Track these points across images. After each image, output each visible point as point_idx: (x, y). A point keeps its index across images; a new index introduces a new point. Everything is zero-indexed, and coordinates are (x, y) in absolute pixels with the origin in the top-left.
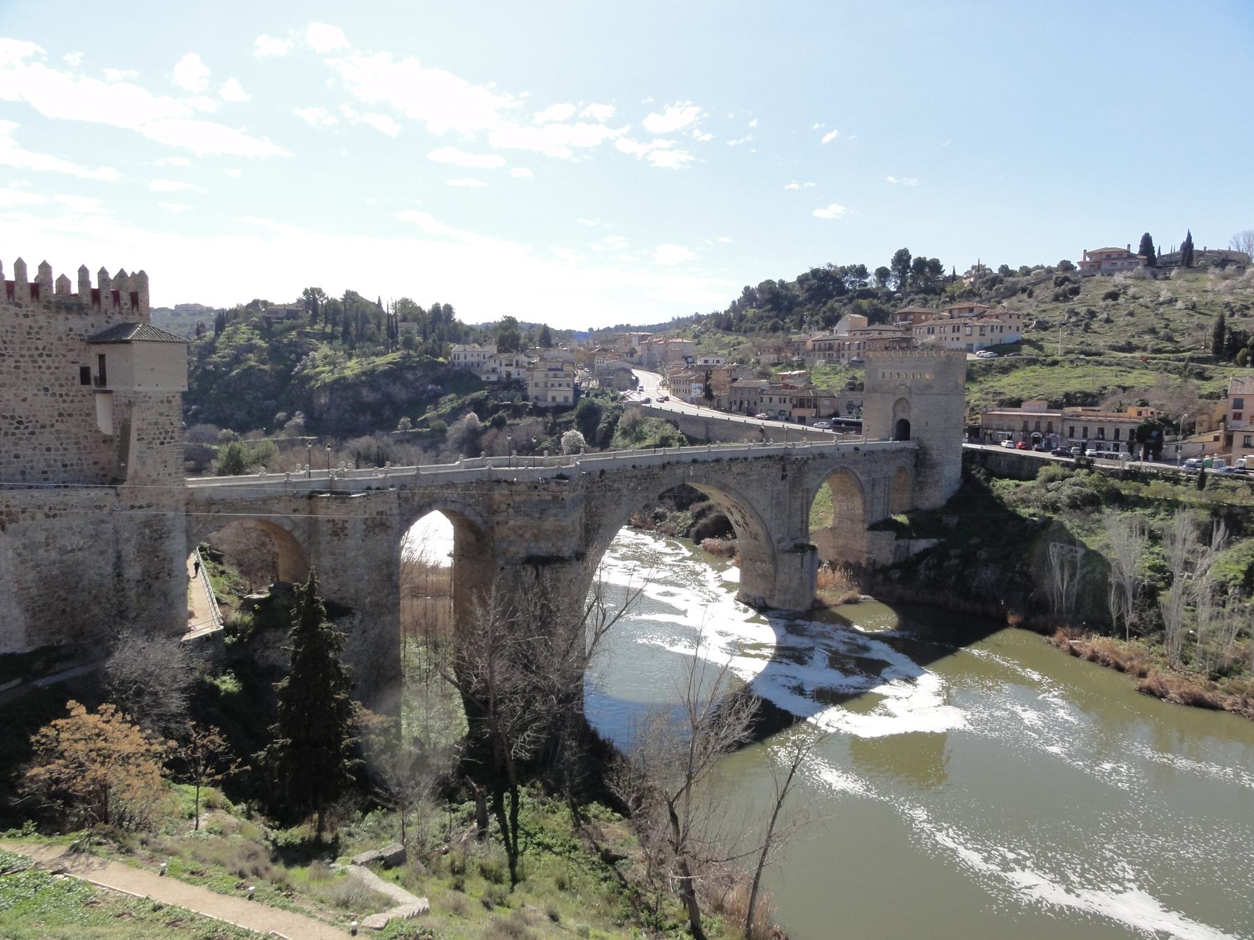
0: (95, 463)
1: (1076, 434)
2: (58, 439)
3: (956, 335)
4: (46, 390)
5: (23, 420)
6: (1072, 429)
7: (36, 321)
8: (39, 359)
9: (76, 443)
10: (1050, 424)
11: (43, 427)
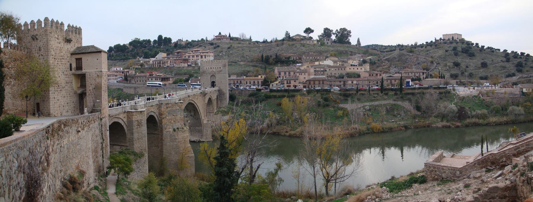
0: (73, 102)
2: (66, 92)
3: (197, 58)
4: (63, 73)
5: (59, 85)
7: (61, 45)
8: (62, 60)
9: (70, 94)
10: (241, 81)
11: (63, 88)
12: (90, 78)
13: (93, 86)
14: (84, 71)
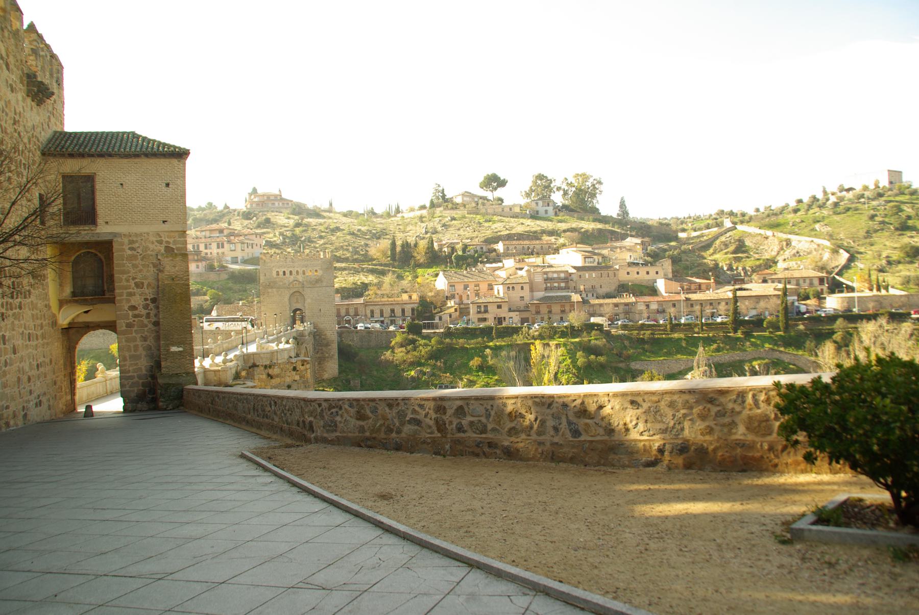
0: (51, 361)
1: (375, 315)
3: (220, 251)
6: (372, 312)
10: (356, 309)
12: (132, 258)
13: (149, 293)
14: (103, 229)
